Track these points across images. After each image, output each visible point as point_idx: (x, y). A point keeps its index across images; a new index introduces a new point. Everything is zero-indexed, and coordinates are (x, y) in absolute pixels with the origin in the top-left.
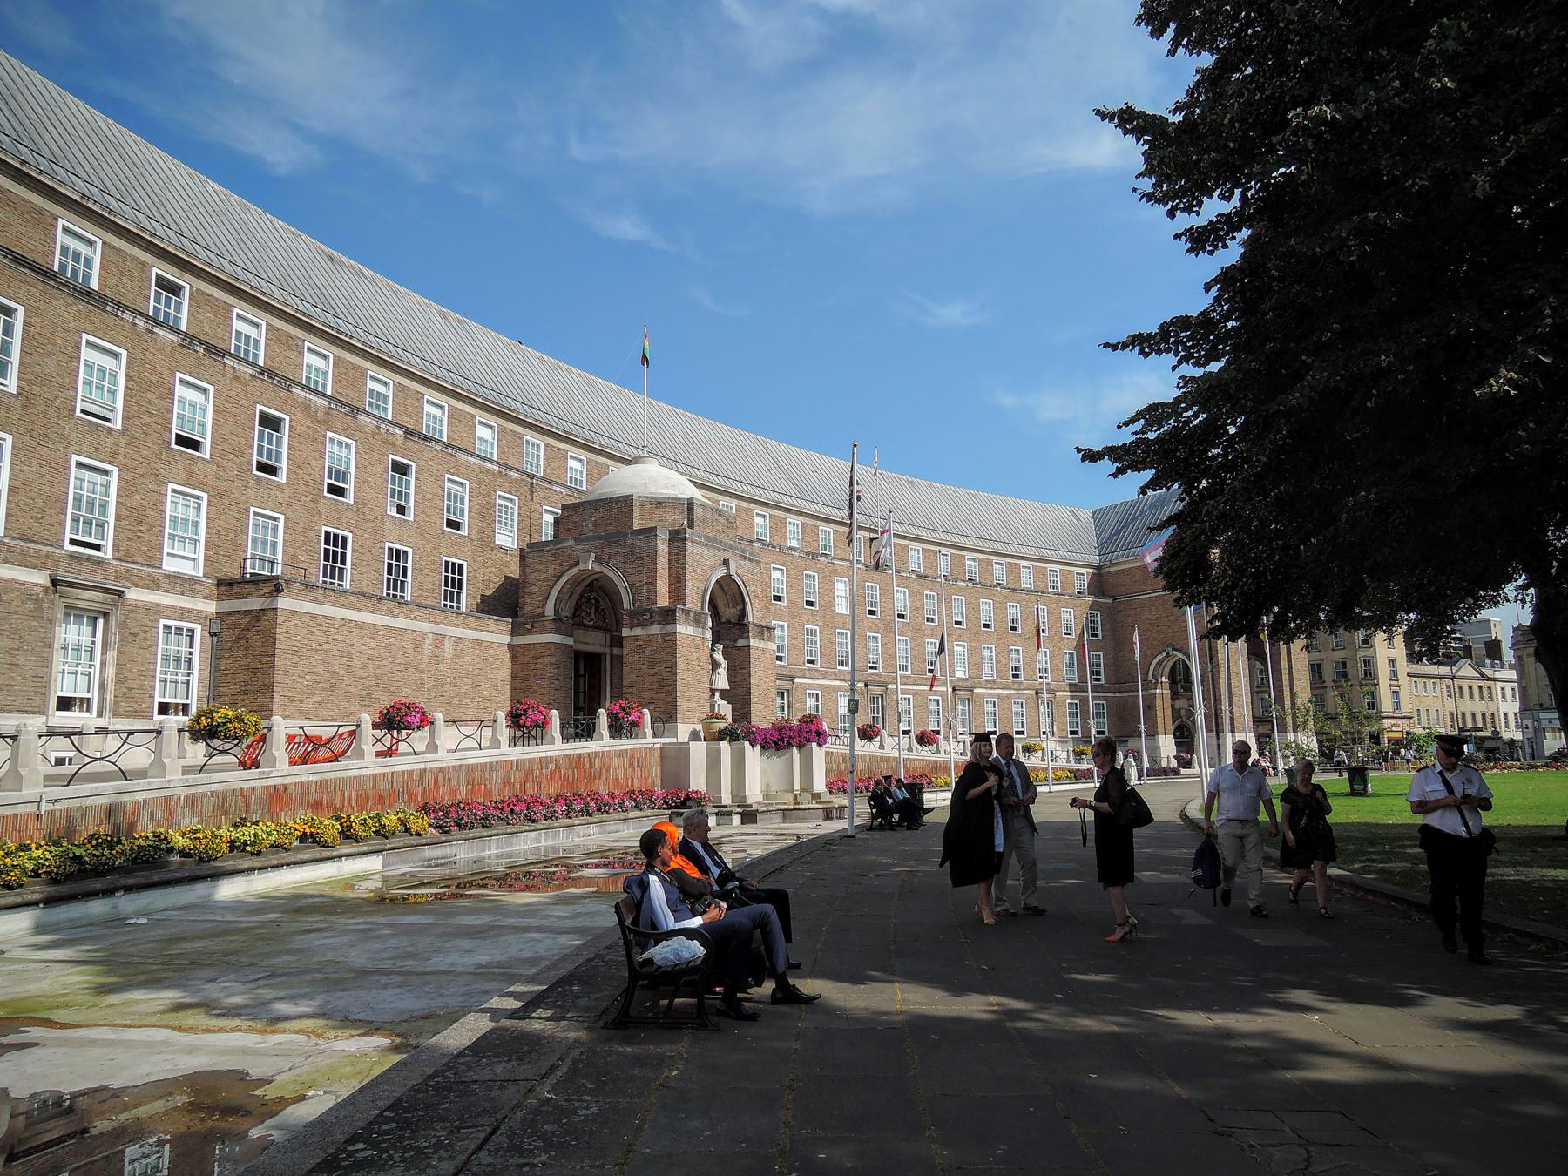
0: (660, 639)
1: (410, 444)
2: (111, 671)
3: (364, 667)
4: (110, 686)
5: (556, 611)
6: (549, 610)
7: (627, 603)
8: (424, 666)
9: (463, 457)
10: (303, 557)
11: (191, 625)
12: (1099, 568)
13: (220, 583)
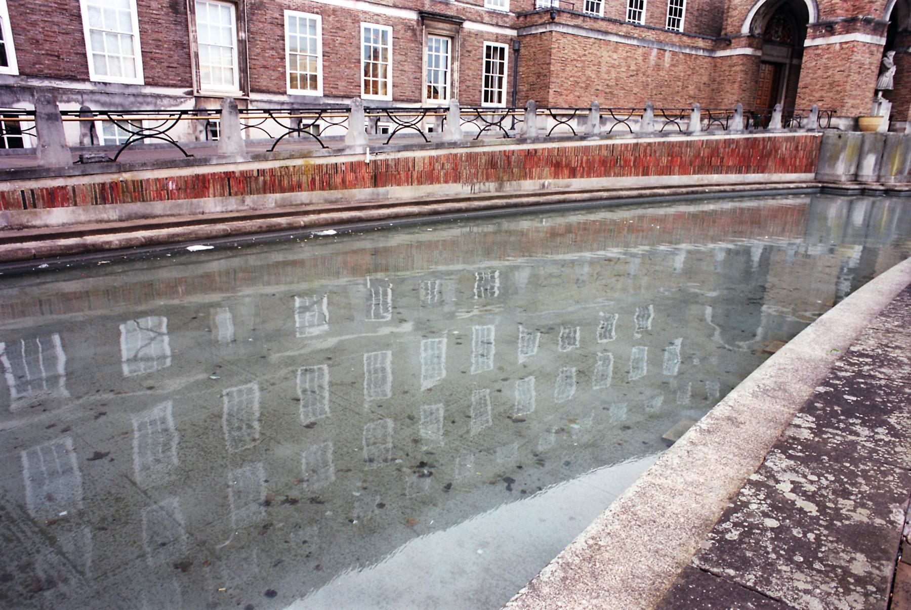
0: (838, 47)
2: (456, 76)
3: (608, 72)
4: (457, 84)
5: (751, 29)
6: (745, 30)
7: (812, 19)
8: (649, 72)
11: (502, 45)
13: (519, 15)
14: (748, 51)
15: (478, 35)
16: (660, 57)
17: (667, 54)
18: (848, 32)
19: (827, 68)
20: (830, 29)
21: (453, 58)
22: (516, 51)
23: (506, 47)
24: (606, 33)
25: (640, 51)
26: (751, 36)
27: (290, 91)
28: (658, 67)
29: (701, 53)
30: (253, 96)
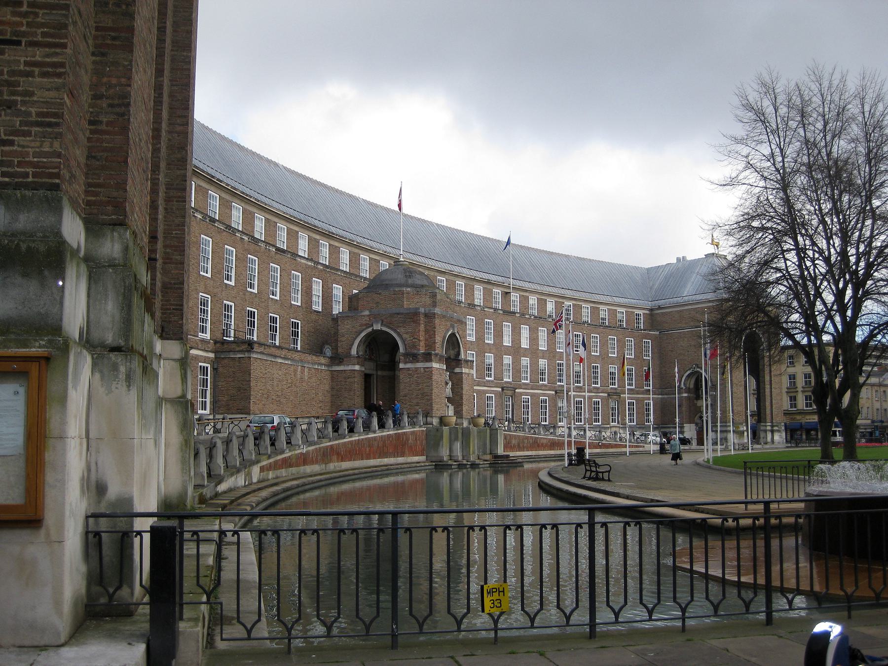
1: (278, 256)
6: (354, 352)
10: (240, 326)
12: (651, 310)
13: (216, 342)
14: (357, 367)
15: (197, 358)
16: (303, 372)
17: (306, 370)
18: (427, 361)
19: (418, 384)
20: (413, 357)
22: (215, 369)
24: (275, 357)
25: (292, 368)
29: (323, 368)
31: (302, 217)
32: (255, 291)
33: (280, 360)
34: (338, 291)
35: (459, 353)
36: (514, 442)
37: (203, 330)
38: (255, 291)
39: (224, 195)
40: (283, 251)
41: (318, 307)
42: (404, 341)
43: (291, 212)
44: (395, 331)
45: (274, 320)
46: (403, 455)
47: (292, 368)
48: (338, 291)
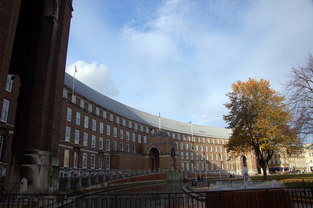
6: (148, 153)
7: (160, 152)
9: (134, 130)
13: (111, 151)
14: (149, 157)
15: (106, 155)
16: (134, 158)
20: (163, 154)
21: (102, 160)
22: (111, 158)
23: (109, 157)
24: (126, 155)
26: (149, 154)
27: (91, 168)
28: (134, 160)
30: (79, 169)
31: (135, 120)
32: (122, 138)
33: (128, 156)
34: (145, 138)
35: (175, 153)
36: (192, 175)
37: (101, 147)
38: (122, 138)
39: (114, 115)
40: (130, 128)
41: (140, 142)
42: (160, 150)
43: (133, 119)
44: (158, 148)
45: (127, 146)
46: (159, 179)
47: (131, 158)
48: (145, 138)
